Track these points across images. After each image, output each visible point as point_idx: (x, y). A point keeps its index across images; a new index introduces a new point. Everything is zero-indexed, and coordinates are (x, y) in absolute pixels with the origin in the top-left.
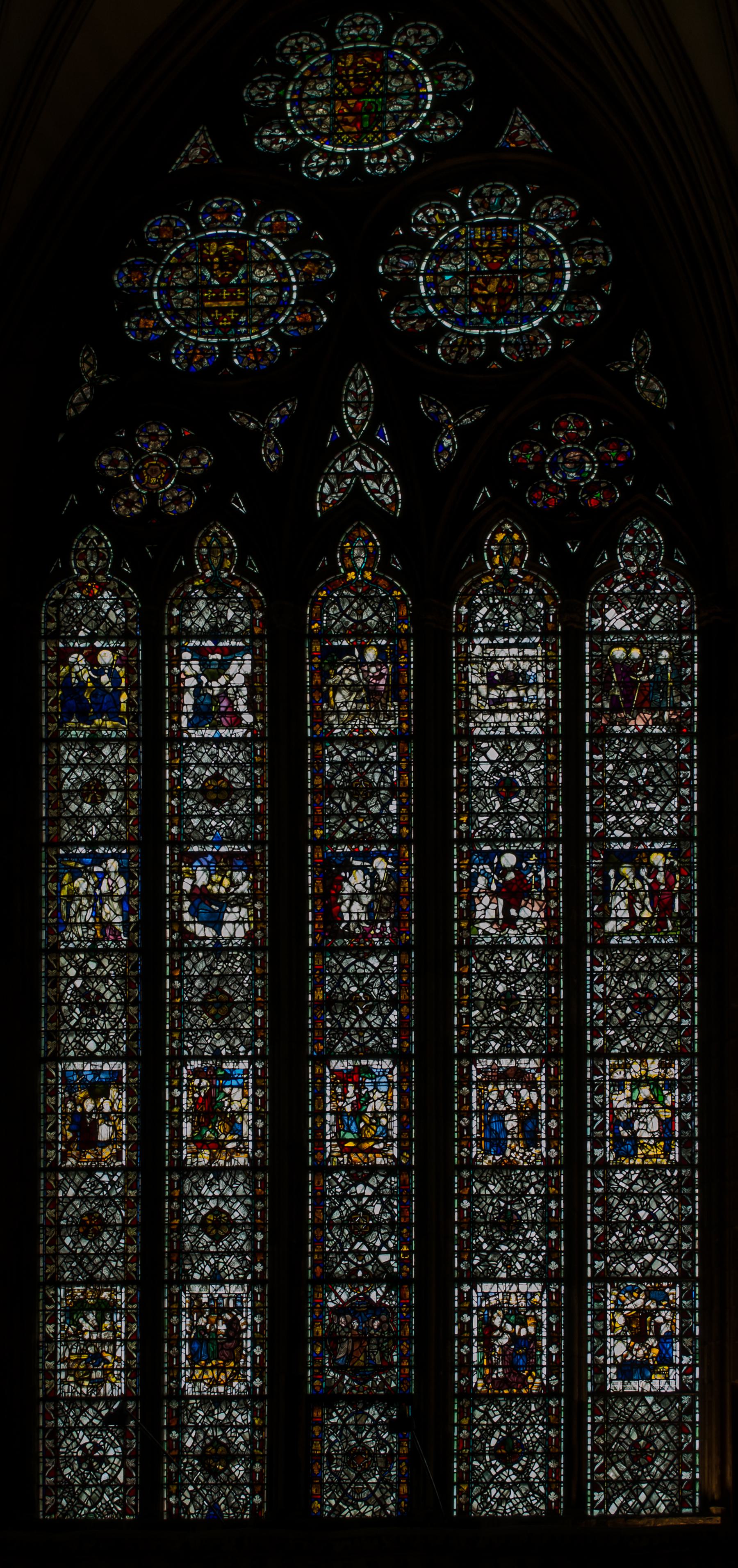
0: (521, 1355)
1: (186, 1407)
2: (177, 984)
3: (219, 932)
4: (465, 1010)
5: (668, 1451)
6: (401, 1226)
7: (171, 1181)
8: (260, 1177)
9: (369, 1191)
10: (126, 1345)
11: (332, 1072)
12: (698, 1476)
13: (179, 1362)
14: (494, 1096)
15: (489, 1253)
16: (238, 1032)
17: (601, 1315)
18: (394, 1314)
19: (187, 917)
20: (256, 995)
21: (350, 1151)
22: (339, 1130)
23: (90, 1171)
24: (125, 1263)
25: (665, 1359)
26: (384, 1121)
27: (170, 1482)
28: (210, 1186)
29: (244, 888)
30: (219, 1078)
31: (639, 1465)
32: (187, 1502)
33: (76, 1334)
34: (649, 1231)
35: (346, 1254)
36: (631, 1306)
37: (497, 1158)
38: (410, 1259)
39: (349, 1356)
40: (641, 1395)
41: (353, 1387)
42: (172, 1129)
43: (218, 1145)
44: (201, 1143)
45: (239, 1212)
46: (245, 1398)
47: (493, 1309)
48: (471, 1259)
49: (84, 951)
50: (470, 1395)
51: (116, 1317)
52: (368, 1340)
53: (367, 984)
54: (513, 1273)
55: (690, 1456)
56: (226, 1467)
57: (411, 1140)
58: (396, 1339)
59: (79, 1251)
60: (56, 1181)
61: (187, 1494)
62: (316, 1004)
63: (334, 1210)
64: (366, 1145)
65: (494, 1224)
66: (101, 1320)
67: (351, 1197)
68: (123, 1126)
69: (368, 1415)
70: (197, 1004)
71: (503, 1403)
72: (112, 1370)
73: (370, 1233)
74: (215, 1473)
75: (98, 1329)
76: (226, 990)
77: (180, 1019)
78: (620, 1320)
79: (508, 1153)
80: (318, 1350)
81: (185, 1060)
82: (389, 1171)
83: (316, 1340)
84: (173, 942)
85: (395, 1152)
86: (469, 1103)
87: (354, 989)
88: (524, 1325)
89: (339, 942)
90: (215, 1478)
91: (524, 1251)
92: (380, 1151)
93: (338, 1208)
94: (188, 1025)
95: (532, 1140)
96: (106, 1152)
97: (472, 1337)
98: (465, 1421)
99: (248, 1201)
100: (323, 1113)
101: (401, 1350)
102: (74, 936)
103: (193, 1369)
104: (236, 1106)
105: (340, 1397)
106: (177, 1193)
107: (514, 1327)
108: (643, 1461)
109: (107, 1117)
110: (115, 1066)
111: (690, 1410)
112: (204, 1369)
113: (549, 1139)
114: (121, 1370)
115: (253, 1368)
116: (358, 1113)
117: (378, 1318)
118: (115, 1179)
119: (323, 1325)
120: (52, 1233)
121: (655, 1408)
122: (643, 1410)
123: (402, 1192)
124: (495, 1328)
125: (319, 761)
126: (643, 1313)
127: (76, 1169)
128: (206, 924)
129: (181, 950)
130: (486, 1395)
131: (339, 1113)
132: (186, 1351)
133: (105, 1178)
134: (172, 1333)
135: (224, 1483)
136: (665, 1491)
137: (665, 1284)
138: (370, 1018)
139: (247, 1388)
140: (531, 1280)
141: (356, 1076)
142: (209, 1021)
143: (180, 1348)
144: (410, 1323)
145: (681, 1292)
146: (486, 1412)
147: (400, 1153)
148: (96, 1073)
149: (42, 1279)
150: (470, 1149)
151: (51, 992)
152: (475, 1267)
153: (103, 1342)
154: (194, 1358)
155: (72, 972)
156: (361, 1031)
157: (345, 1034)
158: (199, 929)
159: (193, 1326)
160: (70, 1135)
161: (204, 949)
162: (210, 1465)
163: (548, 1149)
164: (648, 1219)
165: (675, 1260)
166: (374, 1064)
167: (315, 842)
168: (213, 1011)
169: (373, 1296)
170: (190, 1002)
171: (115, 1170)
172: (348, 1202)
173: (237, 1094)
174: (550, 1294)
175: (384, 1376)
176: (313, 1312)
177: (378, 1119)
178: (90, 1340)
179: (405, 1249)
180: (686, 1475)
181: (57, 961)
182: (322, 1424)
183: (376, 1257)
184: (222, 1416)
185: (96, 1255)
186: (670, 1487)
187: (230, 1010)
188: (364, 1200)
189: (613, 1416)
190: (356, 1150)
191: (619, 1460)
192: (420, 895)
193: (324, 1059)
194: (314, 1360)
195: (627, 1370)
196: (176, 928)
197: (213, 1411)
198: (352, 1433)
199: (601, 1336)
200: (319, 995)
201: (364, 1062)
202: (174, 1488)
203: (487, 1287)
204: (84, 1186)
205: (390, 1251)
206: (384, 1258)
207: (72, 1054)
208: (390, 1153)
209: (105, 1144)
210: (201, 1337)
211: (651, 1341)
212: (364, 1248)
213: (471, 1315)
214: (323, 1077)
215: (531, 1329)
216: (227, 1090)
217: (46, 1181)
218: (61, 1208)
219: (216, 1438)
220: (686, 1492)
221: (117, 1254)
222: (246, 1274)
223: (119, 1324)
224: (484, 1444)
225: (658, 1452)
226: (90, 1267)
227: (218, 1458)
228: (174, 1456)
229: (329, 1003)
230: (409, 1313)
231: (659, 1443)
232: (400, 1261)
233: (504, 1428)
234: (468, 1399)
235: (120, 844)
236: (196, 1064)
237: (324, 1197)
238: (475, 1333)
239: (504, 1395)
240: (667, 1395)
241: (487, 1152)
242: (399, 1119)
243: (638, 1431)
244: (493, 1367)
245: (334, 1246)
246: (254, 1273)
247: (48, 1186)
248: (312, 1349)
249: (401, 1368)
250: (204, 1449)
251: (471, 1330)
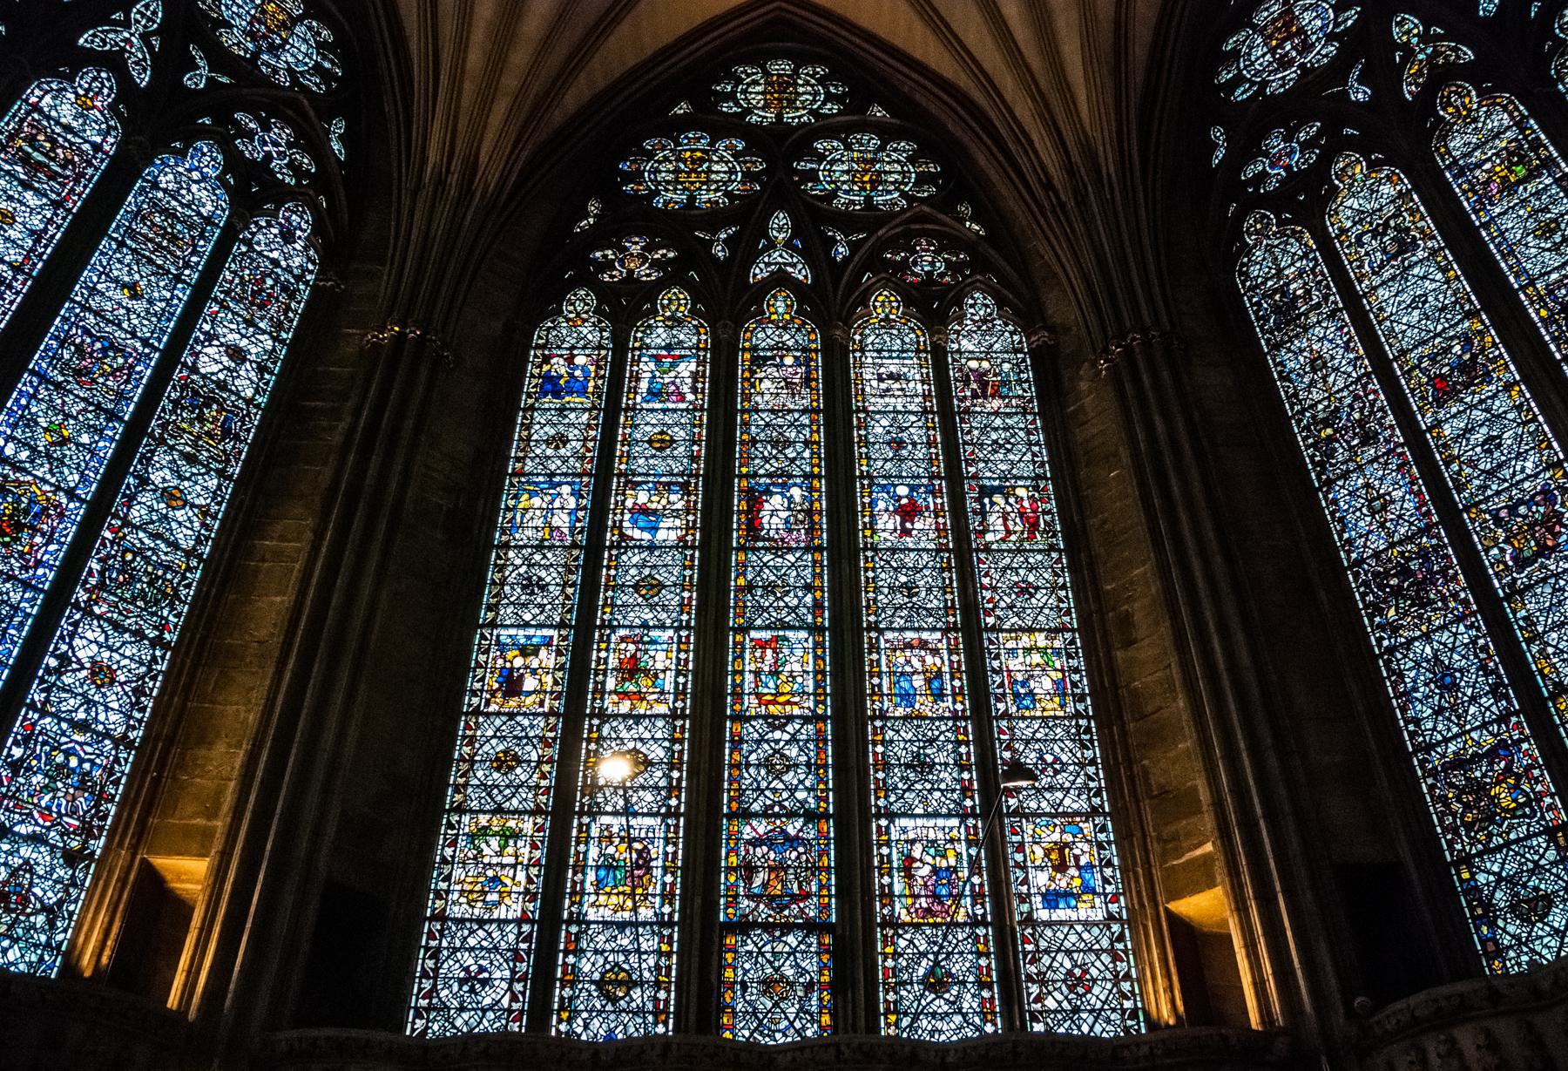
0: (943, 885)
1: (586, 932)
2: (613, 572)
3: (654, 536)
4: (871, 595)
5: (1104, 979)
6: (818, 767)
7: (591, 726)
8: (679, 723)
9: (786, 737)
10: (527, 870)
11: (752, 640)
12: (1139, 1005)
13: (583, 888)
14: (902, 660)
15: (905, 791)
16: (665, 608)
17: (1020, 848)
18: (811, 845)
19: (626, 524)
20: (684, 580)
21: (769, 702)
22: (757, 686)
23: (511, 716)
24: (536, 795)
25: (1088, 889)
26: (799, 680)
27: (562, 1008)
28: (629, 729)
29: (679, 505)
30: (644, 643)
31: (1077, 994)
32: (579, 1030)
33: (475, 858)
34: (1056, 772)
35: (762, 791)
36: (1048, 839)
37: (908, 710)
38: (827, 797)
39: (765, 885)
40: (1071, 924)
41: (770, 916)
42: (596, 682)
43: (641, 697)
44: (625, 695)
45: (657, 753)
46: (651, 924)
47: (913, 842)
48: (886, 797)
49: (532, 547)
50: (892, 923)
51: (520, 843)
52: (785, 870)
53: (785, 574)
54: (930, 809)
55: (1129, 983)
56: (627, 994)
57: (826, 694)
58: (815, 869)
59: (490, 783)
60: (476, 723)
61: (580, 1021)
62: (739, 589)
63: (751, 752)
64: (781, 699)
65: (908, 766)
66: (503, 847)
67: (767, 741)
68: (549, 679)
69: (786, 943)
70: (629, 586)
71: (928, 932)
72: (510, 893)
73: (787, 772)
74: (614, 1000)
75: (500, 854)
76: (657, 576)
77: (612, 598)
78: (1039, 852)
79: (917, 706)
80: (732, 879)
81: (613, 629)
82: (806, 720)
83: (730, 869)
84: (612, 542)
85: (811, 705)
86: (879, 665)
87: (773, 578)
88: (944, 856)
89: (760, 544)
90: (613, 1005)
91: (939, 789)
92: (796, 703)
93: (755, 751)
94: (619, 602)
95: (939, 696)
96: (529, 700)
97: (891, 868)
98: (889, 950)
99: (666, 744)
100: (742, 673)
101: (820, 880)
102: (525, 536)
103: (597, 894)
104: (659, 666)
105: (755, 925)
106: (595, 735)
107: (934, 858)
108: (1081, 990)
109: (534, 672)
110: (547, 632)
111: (1121, 938)
112: (609, 894)
113: (954, 694)
114: (519, 893)
115: (663, 896)
116: (775, 673)
117: (795, 850)
118: (535, 722)
119: (737, 855)
120: (464, 767)
121: (1086, 936)
122: (1073, 938)
123: (820, 738)
124: (914, 860)
125: (746, 424)
126: (1062, 847)
127: (498, 714)
128: (642, 529)
129: (619, 547)
130: (911, 924)
131: (757, 673)
132: (591, 876)
133: (526, 722)
134: (578, 860)
135: (624, 1010)
136: (1108, 1021)
137: (1078, 819)
138: (787, 599)
139: (656, 914)
140: (949, 815)
141: (774, 644)
142: (640, 600)
143: (584, 874)
144: (828, 855)
145: (1095, 826)
146: (911, 941)
147: (816, 706)
148: (528, 637)
149: (447, 807)
150: (882, 703)
151: (497, 576)
152: (891, 804)
153: (503, 866)
154: (599, 884)
155: (518, 562)
156: (777, 609)
157: (764, 611)
158: (637, 534)
159: (601, 854)
160: (496, 686)
161: (640, 547)
162: (608, 991)
163: (954, 702)
164: (1054, 762)
165: (1084, 797)
166: (789, 634)
167: (741, 476)
168: (644, 592)
169: (791, 831)
170: (623, 585)
171: (536, 715)
172: (766, 746)
173: (661, 656)
174: (967, 828)
175: (802, 905)
176: (728, 844)
177: (794, 678)
178: (489, 864)
179: (822, 786)
180: (1128, 1004)
181: (506, 554)
182: (736, 952)
183: (792, 794)
184: (625, 942)
185: (507, 786)
186: (1112, 1017)
187: (660, 592)
188: (782, 743)
189: (1043, 944)
190: (774, 702)
191: (1055, 989)
192: (832, 513)
193: (743, 630)
194: (728, 889)
195: (1052, 899)
196: (616, 532)
197: (616, 937)
198: (768, 961)
199: (1023, 867)
200: (741, 581)
201: (781, 633)
202: (565, 1015)
203: (904, 822)
204: (504, 728)
205: (808, 790)
206: (801, 795)
207: (508, 622)
208: (806, 705)
209: (529, 693)
210: (609, 865)
211: (1073, 871)
212: (781, 786)
213: (890, 847)
214: (742, 644)
215: (952, 862)
216: (652, 653)
217: (466, 722)
218: (477, 745)
219: (617, 964)
220: (1129, 1023)
221: (529, 788)
222: (660, 807)
223: (522, 851)
224: (911, 974)
225: (1094, 981)
226: (499, 798)
227: (620, 983)
228: (568, 981)
229: (750, 587)
230: (827, 845)
231: (1094, 972)
232: (817, 798)
233: (931, 957)
234: (892, 928)
235: (574, 475)
236: (622, 632)
237: (741, 741)
238: (895, 865)
239: (928, 924)
240: (1096, 924)
241: (896, 706)
242: (815, 677)
243: (1072, 959)
244: (916, 897)
245: (751, 784)
246: (669, 807)
247: (467, 727)
248: (726, 878)
249: (820, 896)
250: (603, 975)
251: (890, 861)
